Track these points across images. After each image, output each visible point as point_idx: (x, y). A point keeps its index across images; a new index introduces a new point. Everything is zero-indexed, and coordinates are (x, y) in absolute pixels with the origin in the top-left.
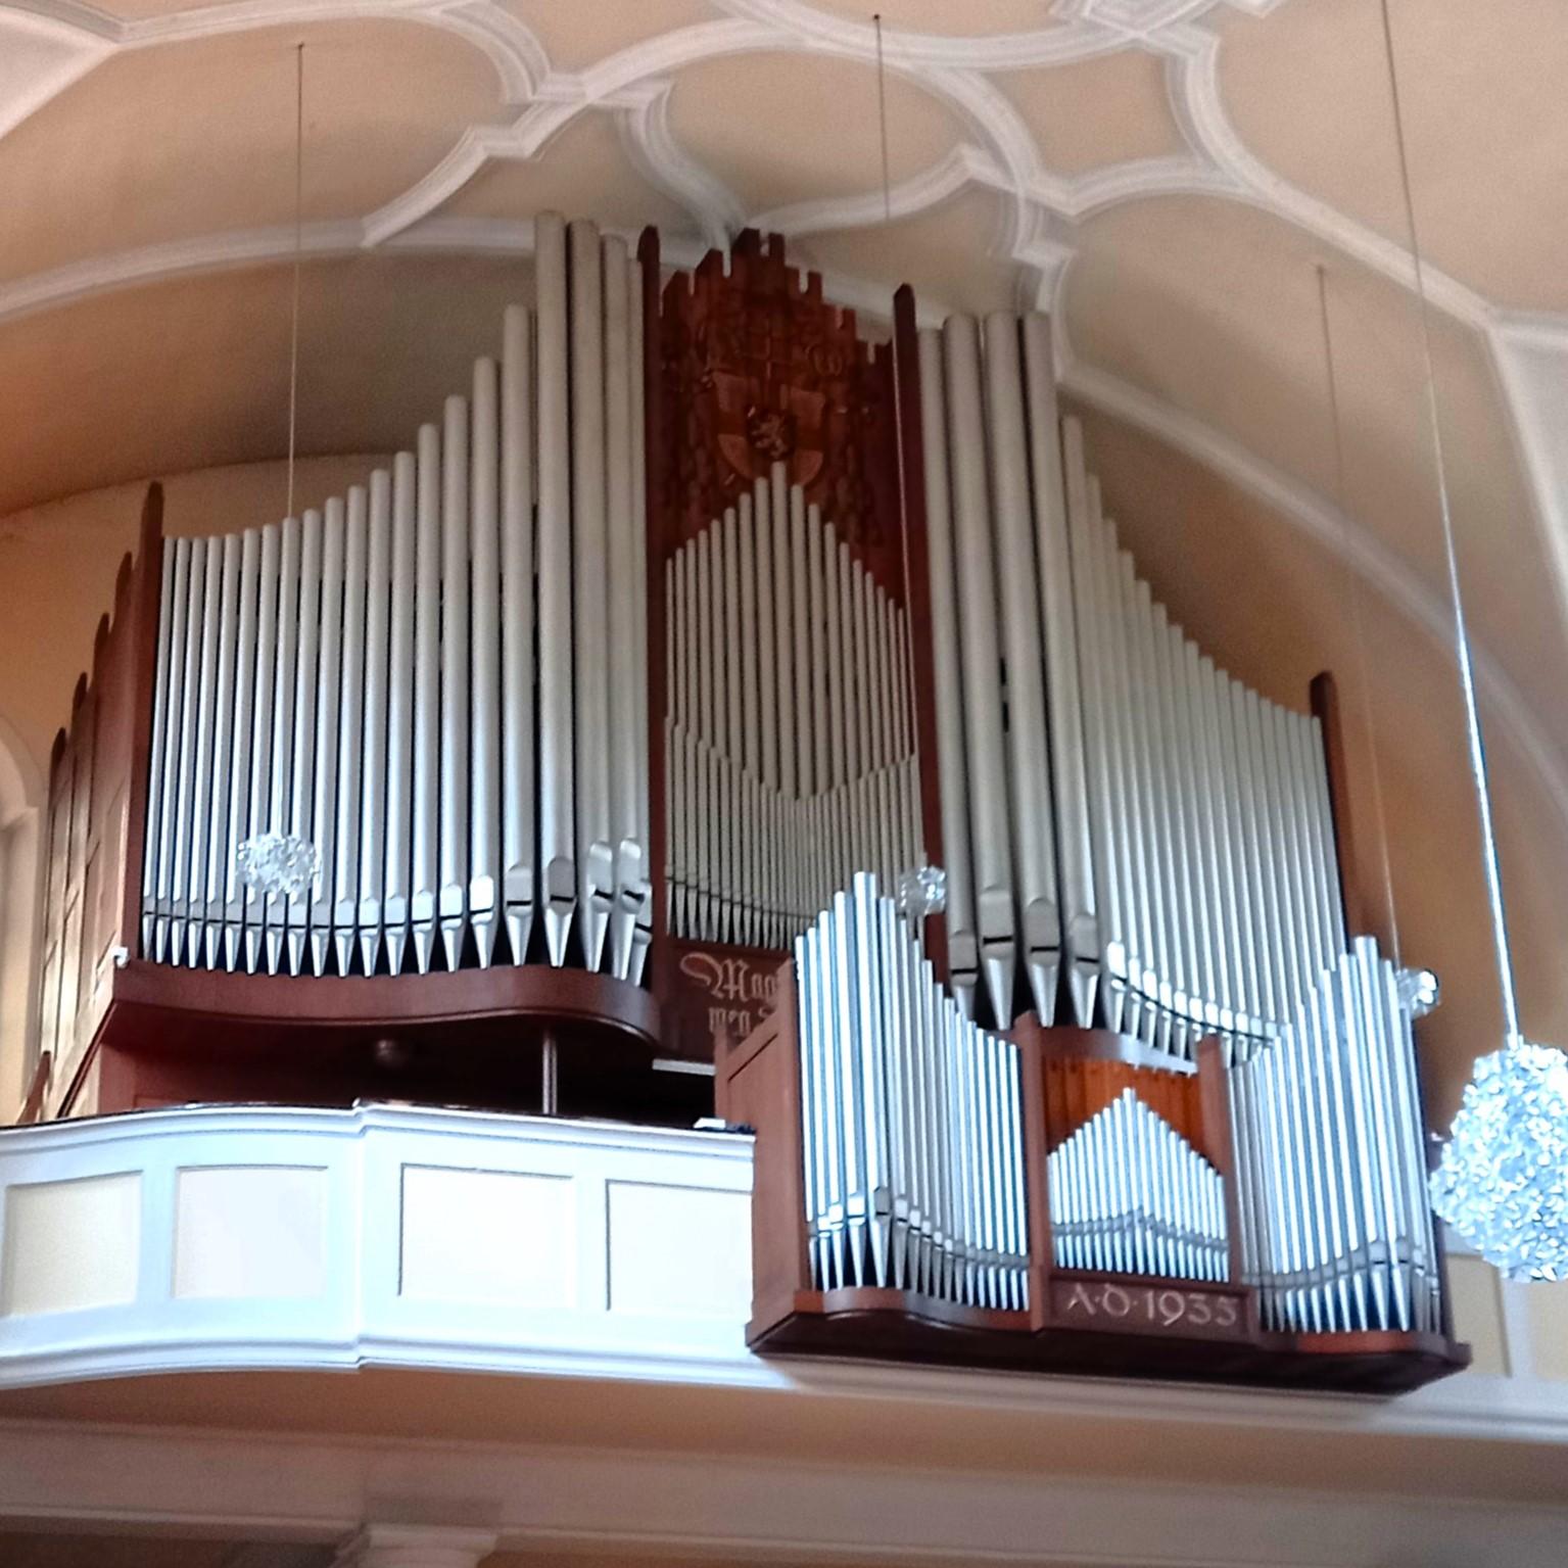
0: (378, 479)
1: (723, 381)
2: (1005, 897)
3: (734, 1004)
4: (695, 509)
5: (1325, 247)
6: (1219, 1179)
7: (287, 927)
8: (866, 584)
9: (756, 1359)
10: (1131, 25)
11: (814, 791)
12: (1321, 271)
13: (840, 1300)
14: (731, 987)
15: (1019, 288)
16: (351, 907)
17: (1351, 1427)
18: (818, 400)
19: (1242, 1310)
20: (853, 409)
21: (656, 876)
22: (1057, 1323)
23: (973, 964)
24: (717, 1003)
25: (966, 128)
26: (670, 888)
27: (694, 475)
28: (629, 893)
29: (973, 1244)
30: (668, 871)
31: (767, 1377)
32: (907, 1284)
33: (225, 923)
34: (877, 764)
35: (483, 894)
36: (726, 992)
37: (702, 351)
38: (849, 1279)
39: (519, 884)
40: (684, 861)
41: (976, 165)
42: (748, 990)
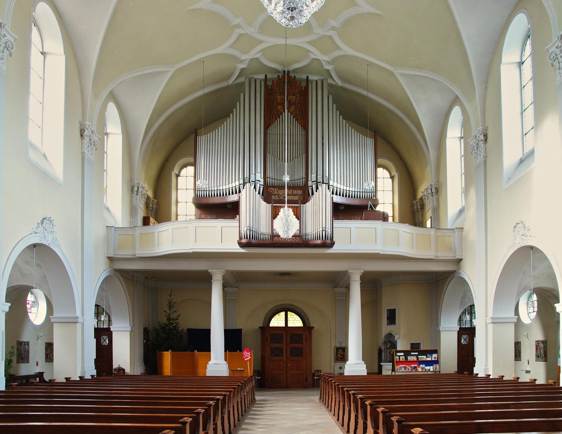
0: (225, 123)
1: (279, 97)
2: (315, 175)
3: (276, 195)
4: (274, 118)
5: (367, 61)
6: (299, 221)
7: (214, 190)
8: (299, 126)
9: (240, 248)
10: (323, 32)
11: (290, 161)
12: (368, 64)
13: (244, 241)
14: (275, 192)
15: (328, 71)
16: (214, 188)
17: (325, 252)
18: (295, 97)
19: (300, 239)
20: (300, 98)
21: (265, 178)
22: (273, 242)
23: (311, 185)
24: (273, 195)
25: (309, 51)
26: (267, 178)
27: (274, 113)
28: (258, 180)
29: (267, 232)
30: (267, 176)
31: (243, 250)
32: (252, 238)
33: (204, 191)
34: (296, 157)
35: (237, 183)
36: (274, 193)
37: (276, 94)
38: (245, 238)
39: (242, 182)
40: (269, 174)
41: (313, 56)
42: (278, 193)
